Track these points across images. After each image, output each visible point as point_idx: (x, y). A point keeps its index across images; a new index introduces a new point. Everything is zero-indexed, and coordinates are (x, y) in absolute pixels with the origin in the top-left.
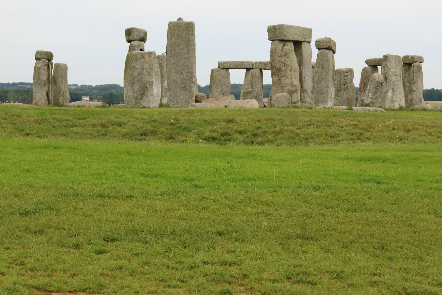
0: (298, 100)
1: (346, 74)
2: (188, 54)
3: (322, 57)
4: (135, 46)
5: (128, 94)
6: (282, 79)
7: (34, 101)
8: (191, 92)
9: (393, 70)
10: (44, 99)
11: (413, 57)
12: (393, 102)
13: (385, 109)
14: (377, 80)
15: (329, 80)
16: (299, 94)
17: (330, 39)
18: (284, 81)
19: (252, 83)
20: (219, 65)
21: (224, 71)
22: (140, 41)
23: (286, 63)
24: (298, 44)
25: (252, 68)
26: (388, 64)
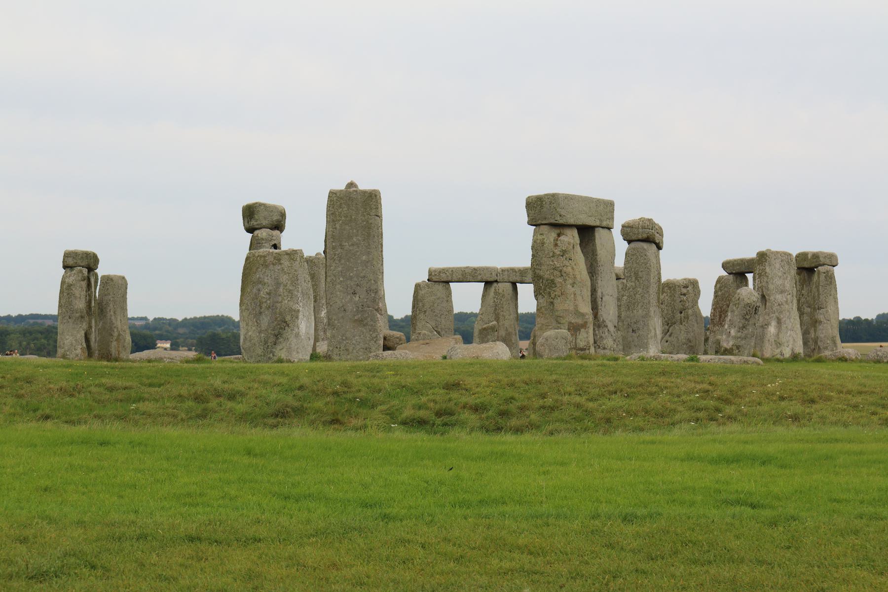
0: (588, 342)
1: (684, 291)
2: (369, 253)
3: (635, 257)
4: (263, 239)
5: (248, 334)
6: (555, 301)
7: (60, 351)
8: (375, 330)
10: (80, 347)
11: (816, 256)
12: (778, 344)
13: (763, 359)
14: (747, 301)
15: (649, 302)
16: (591, 331)
17: (650, 220)
18: (560, 305)
19: (496, 309)
20: (430, 274)
21: (440, 287)
23: (565, 269)
24: (586, 232)
25: (496, 281)
26: (768, 270)
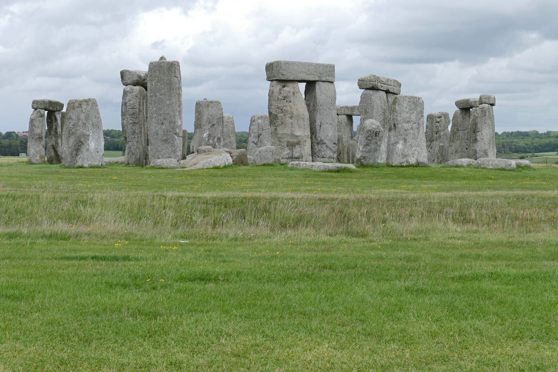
0: (301, 154)
1: (438, 120)
2: (170, 100)
8: (174, 146)
18: (280, 131)
22: (135, 85)
24: (311, 85)
26: (397, 108)
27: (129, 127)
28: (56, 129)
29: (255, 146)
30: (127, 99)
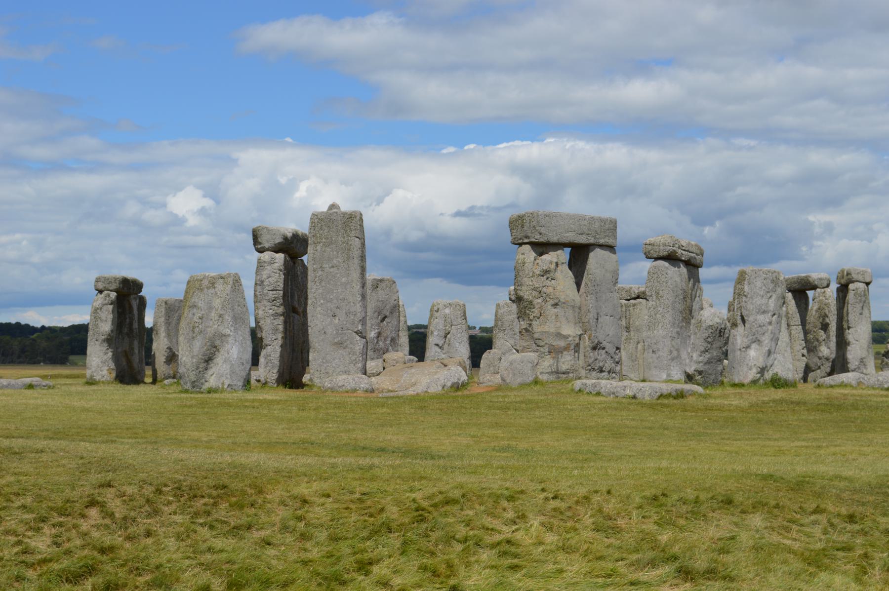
2: (348, 275)
6: (534, 323)
9: (758, 301)
18: (537, 327)
22: (277, 252)
27: (268, 321)
28: (131, 324)
29: (439, 350)
30: (265, 274)
